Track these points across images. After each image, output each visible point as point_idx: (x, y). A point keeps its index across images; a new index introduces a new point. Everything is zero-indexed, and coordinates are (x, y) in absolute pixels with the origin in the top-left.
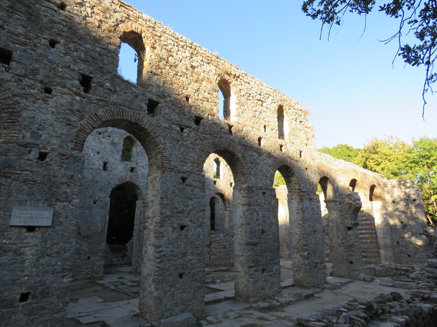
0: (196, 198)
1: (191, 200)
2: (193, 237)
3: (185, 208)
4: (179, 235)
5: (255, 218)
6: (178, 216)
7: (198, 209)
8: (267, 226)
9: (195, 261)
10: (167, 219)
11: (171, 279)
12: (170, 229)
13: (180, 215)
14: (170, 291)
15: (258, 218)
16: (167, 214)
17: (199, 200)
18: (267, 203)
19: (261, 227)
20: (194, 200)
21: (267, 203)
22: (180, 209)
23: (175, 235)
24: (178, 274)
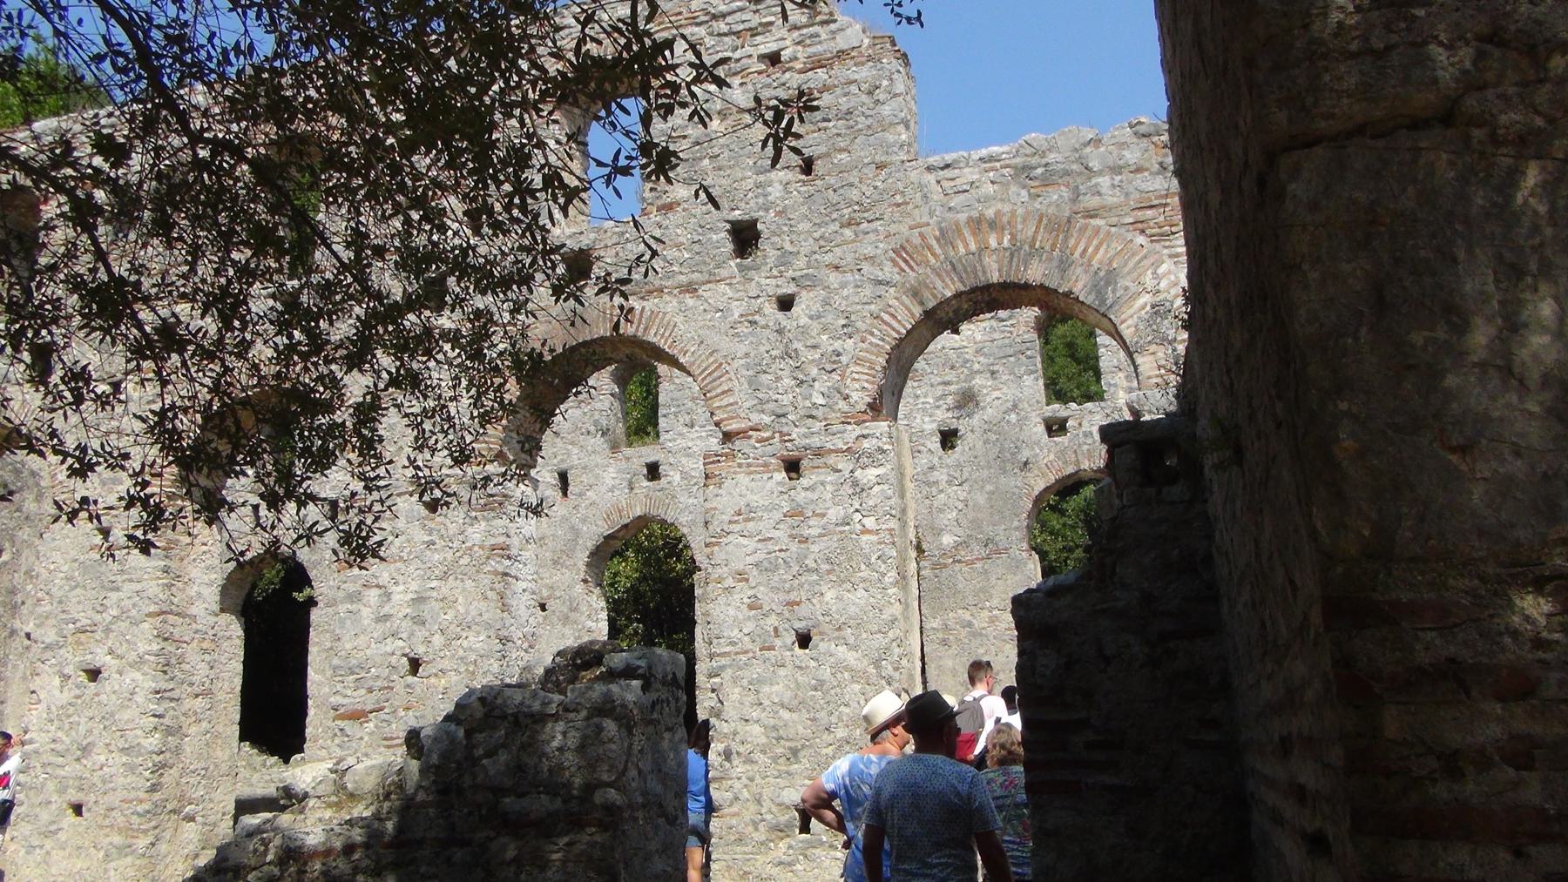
0: (131, 581)
1: (118, 589)
2: (114, 697)
3: (98, 617)
4: (78, 697)
5: (366, 612)
6: (78, 643)
7: (134, 612)
8: (438, 640)
9: (113, 770)
10: (48, 654)
11: (45, 816)
12: (57, 681)
13: (83, 637)
14: (42, 847)
15: (386, 610)
16: (48, 641)
17: (138, 587)
18: (440, 543)
19: (401, 643)
20: (128, 587)
21: (440, 543)
22: (85, 622)
23: (66, 696)
24: (65, 805)
